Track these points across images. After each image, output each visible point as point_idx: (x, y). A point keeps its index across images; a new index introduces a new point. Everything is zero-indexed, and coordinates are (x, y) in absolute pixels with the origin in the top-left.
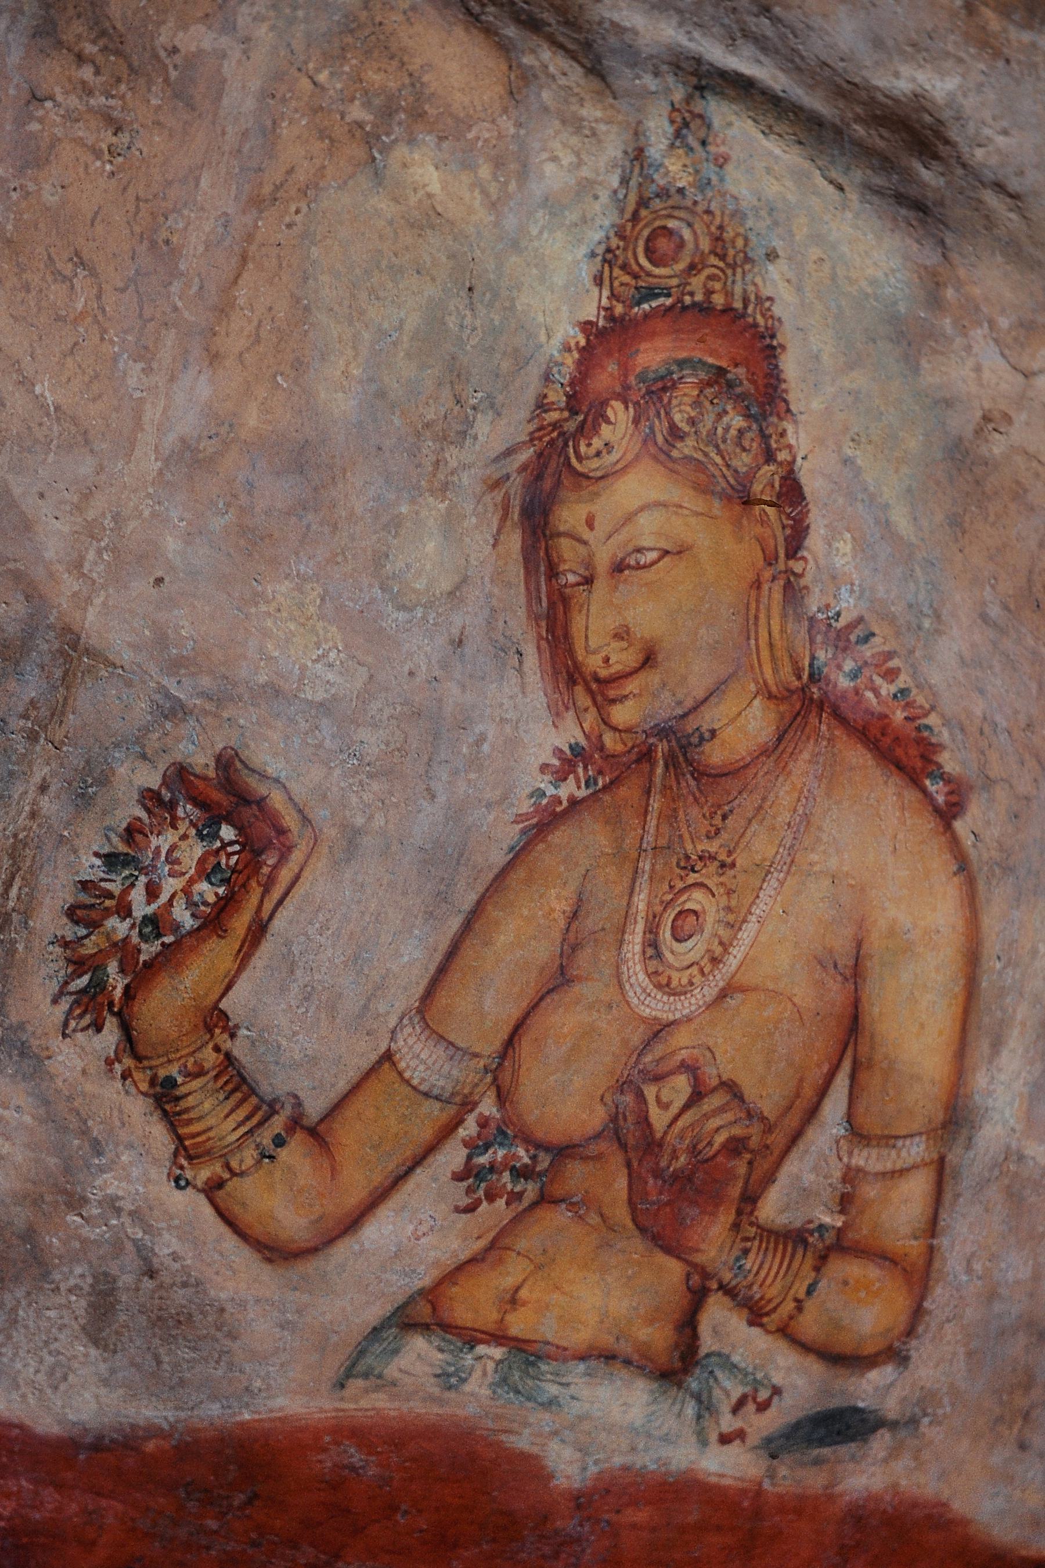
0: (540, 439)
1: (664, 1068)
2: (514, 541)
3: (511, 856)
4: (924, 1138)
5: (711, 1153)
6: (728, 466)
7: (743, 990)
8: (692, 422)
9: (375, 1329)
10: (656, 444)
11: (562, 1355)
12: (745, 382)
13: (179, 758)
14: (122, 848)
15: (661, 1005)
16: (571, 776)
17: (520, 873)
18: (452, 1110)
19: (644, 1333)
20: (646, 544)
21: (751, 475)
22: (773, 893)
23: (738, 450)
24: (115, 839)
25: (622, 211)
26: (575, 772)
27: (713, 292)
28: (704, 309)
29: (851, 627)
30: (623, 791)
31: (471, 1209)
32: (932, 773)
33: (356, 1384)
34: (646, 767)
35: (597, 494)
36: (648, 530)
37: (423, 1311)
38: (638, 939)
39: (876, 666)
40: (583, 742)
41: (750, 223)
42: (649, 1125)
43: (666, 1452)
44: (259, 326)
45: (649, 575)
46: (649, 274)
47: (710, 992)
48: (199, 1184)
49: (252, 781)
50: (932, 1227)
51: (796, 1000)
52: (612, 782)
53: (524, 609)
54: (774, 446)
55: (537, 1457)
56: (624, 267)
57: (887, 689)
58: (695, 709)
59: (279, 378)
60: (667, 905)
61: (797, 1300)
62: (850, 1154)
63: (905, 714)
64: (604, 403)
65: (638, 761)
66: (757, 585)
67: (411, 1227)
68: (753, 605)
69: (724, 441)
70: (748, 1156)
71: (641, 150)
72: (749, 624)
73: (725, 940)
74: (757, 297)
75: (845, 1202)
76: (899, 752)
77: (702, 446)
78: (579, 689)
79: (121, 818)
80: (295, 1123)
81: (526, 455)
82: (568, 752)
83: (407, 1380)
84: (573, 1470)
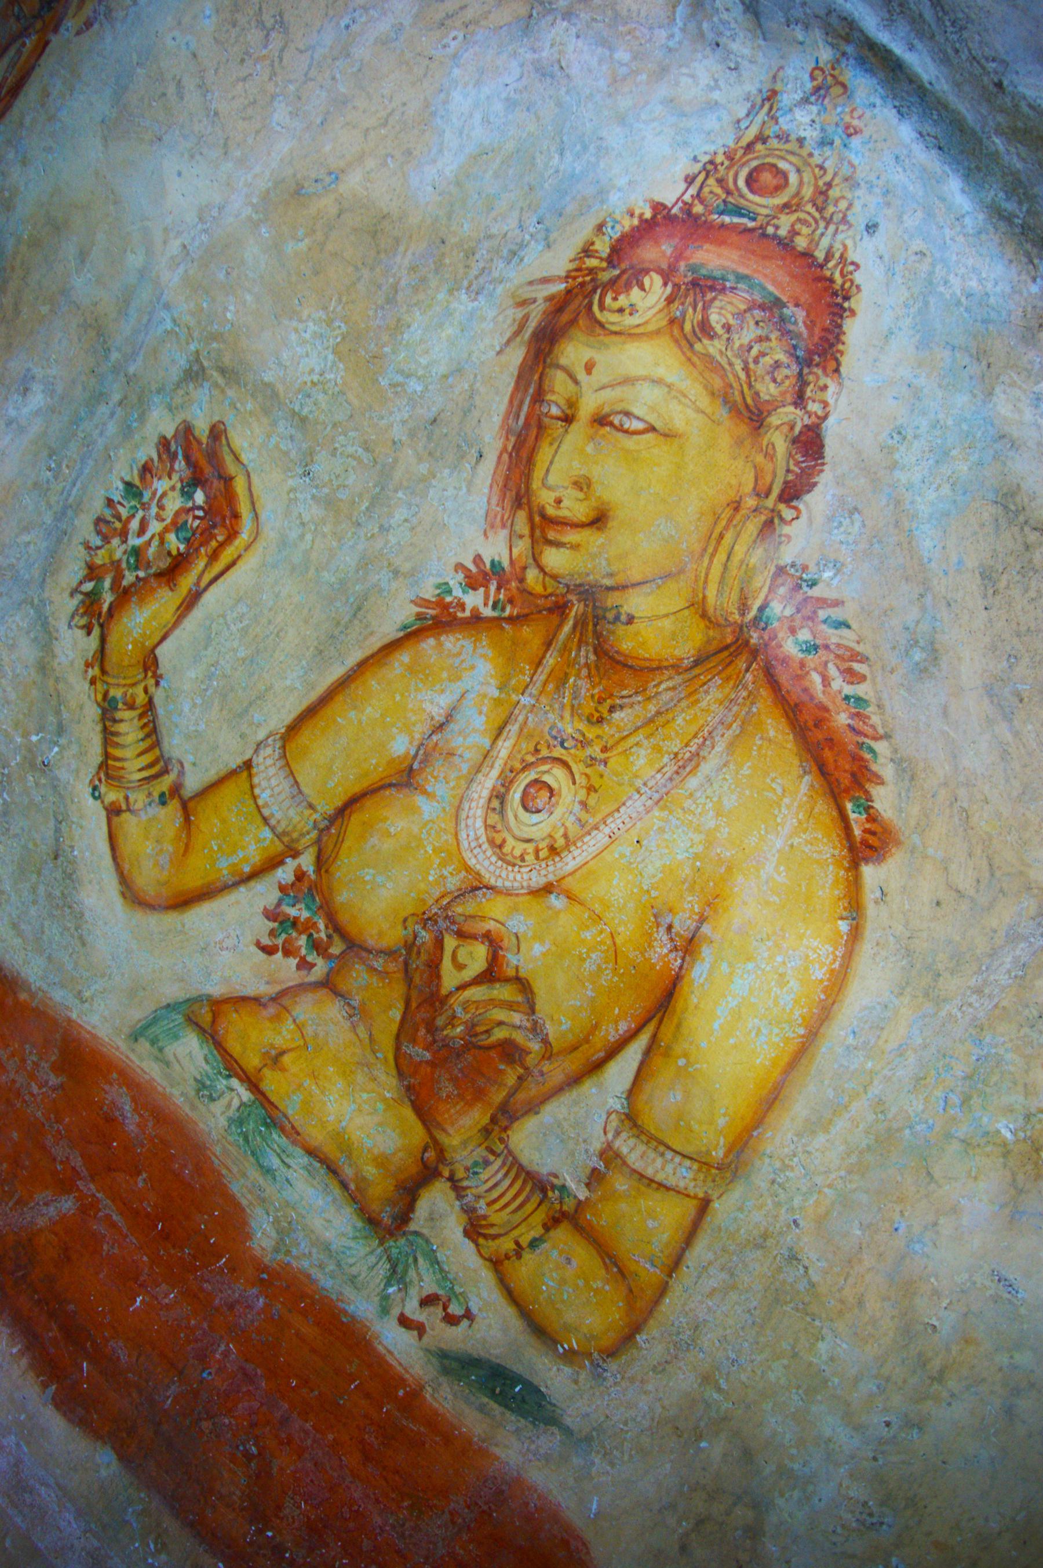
0: (574, 278)
1: (467, 928)
2: (517, 356)
3: (401, 634)
4: (695, 1166)
5: (486, 1042)
6: (750, 386)
8: (728, 328)
9: (168, 1005)
10: (682, 329)
11: (293, 1133)
12: (801, 324)
13: (189, 419)
14: (137, 482)
15: (486, 863)
16: (482, 590)
17: (404, 657)
18: (279, 847)
19: (370, 1171)
20: (636, 411)
21: (774, 406)
22: (634, 815)
23: (768, 378)
24: (136, 472)
25: (738, 139)
26: (487, 587)
27: (798, 234)
28: (786, 245)
29: (823, 602)
30: (526, 631)
31: (269, 950)
32: (858, 799)
33: (144, 1046)
34: (555, 619)
35: (607, 347)
36: (645, 401)
38: (489, 783)
39: (837, 656)
40: (506, 563)
41: (859, 193)
42: (439, 977)
43: (349, 1292)
44: (390, 114)
45: (630, 443)
46: (742, 196)
47: (538, 880)
48: (107, 801)
49: (228, 459)
50: (675, 1264)
52: (518, 617)
53: (500, 418)
54: (808, 394)
55: (243, 1210)
56: (720, 181)
57: (838, 683)
58: (623, 588)
59: (389, 160)
60: (527, 767)
61: (517, 1243)
62: (617, 1133)
63: (850, 721)
64: (647, 272)
65: (550, 611)
66: (736, 506)
67: (220, 937)
68: (724, 523)
69: (756, 361)
70: (521, 1071)
71: (774, 93)
73: (571, 835)
74: (841, 257)
75: (595, 1178)
76: (827, 754)
77: (729, 354)
78: (522, 516)
79: (142, 457)
80: (176, 790)
82: (488, 566)
83: (177, 1067)
84: (268, 1244)
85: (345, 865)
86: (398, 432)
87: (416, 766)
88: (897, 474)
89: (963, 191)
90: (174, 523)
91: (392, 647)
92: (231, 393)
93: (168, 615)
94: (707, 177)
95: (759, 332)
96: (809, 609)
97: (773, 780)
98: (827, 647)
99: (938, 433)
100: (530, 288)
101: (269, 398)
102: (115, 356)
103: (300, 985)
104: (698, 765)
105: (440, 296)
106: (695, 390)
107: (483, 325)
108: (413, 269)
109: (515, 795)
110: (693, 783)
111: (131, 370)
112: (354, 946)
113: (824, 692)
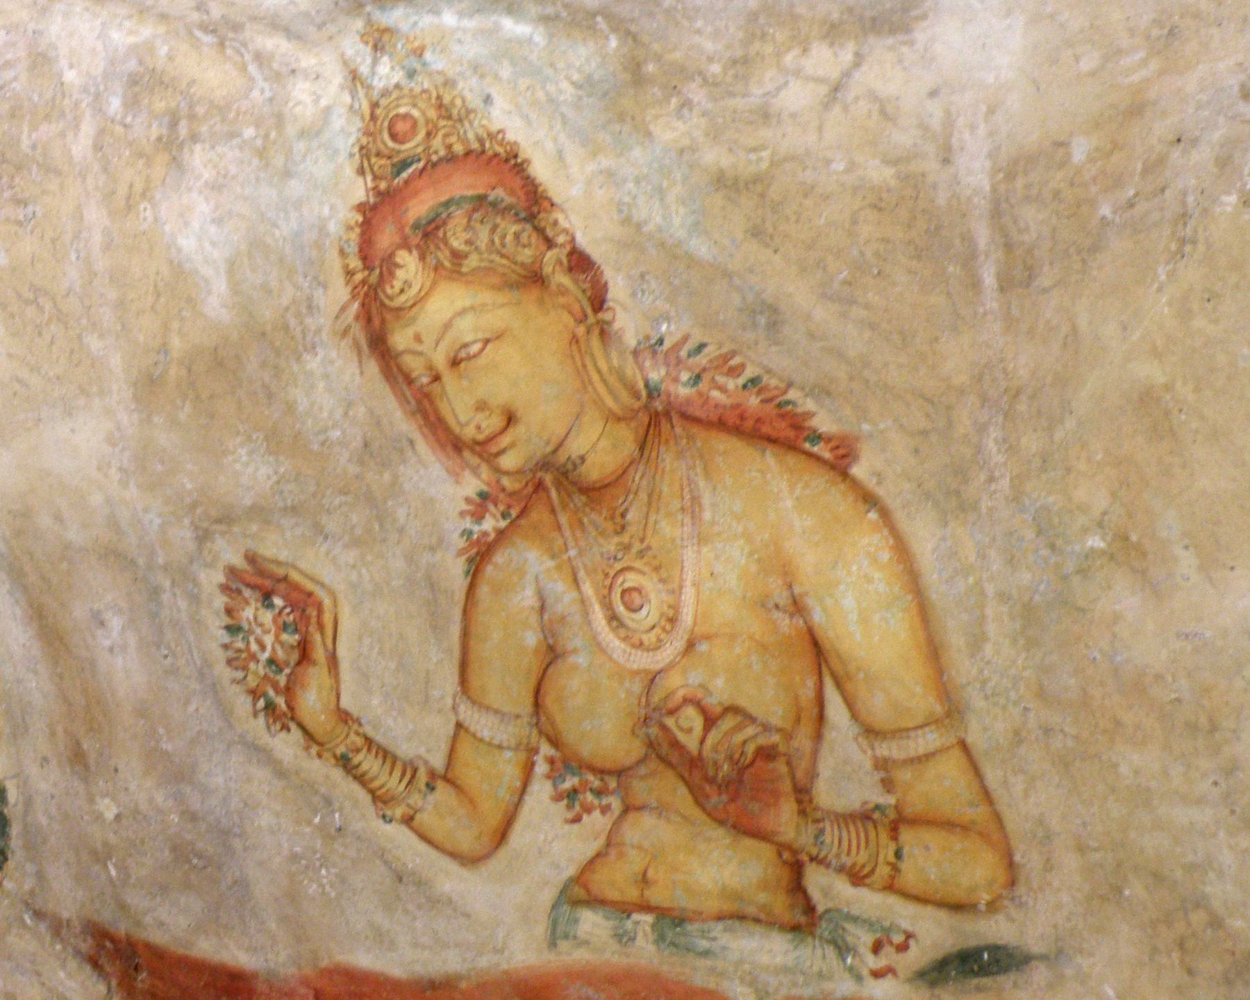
1: (671, 705)
2: (373, 367)
3: (469, 579)
5: (747, 762)
6: (516, 263)
7: (708, 637)
16: (487, 516)
17: (483, 591)
18: (522, 756)
20: (468, 338)
21: (539, 260)
23: (520, 249)
29: (677, 346)
31: (577, 820)
34: (542, 494)
36: (467, 330)
37: (579, 892)
39: (717, 368)
40: (485, 488)
45: (482, 361)
47: (679, 644)
51: (757, 637)
54: (549, 232)
57: (731, 384)
58: (560, 445)
66: (575, 339)
69: (504, 246)
72: (581, 373)
76: (765, 429)
78: (467, 454)
80: (433, 775)
81: (356, 306)
85: (570, 734)
86: (353, 469)
87: (551, 642)
88: (646, 229)
89: (517, 22)
90: (278, 628)
91: (471, 589)
92: (236, 529)
93: (328, 681)
94: (369, 160)
95: (489, 226)
96: (673, 359)
97: (750, 471)
98: (704, 370)
99: (644, 184)
100: (340, 321)
101: (259, 512)
102: (141, 561)
103: (614, 824)
104: (700, 505)
105: (296, 368)
106: (486, 296)
107: (337, 365)
108: (263, 365)
109: (621, 609)
110: (707, 515)
111: (161, 561)
112: (620, 773)
113: (729, 396)
